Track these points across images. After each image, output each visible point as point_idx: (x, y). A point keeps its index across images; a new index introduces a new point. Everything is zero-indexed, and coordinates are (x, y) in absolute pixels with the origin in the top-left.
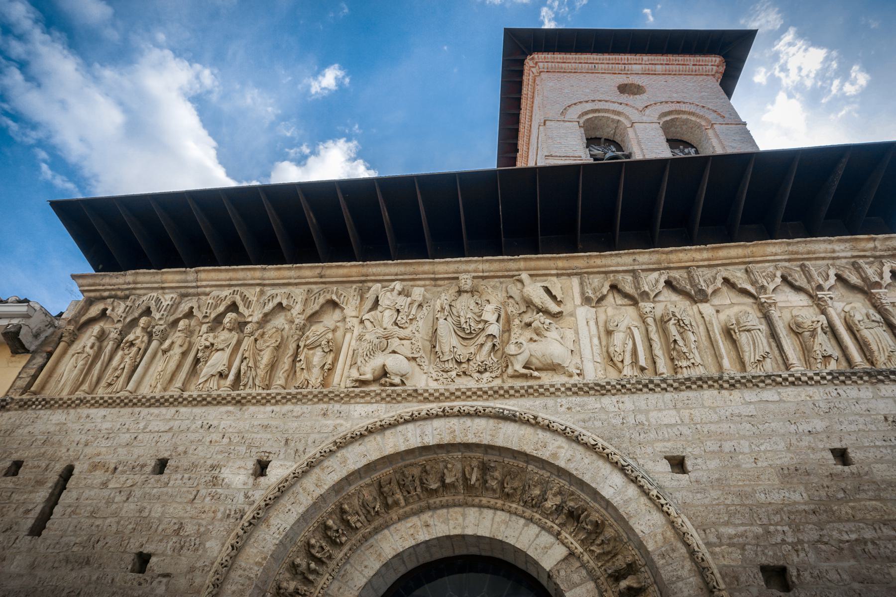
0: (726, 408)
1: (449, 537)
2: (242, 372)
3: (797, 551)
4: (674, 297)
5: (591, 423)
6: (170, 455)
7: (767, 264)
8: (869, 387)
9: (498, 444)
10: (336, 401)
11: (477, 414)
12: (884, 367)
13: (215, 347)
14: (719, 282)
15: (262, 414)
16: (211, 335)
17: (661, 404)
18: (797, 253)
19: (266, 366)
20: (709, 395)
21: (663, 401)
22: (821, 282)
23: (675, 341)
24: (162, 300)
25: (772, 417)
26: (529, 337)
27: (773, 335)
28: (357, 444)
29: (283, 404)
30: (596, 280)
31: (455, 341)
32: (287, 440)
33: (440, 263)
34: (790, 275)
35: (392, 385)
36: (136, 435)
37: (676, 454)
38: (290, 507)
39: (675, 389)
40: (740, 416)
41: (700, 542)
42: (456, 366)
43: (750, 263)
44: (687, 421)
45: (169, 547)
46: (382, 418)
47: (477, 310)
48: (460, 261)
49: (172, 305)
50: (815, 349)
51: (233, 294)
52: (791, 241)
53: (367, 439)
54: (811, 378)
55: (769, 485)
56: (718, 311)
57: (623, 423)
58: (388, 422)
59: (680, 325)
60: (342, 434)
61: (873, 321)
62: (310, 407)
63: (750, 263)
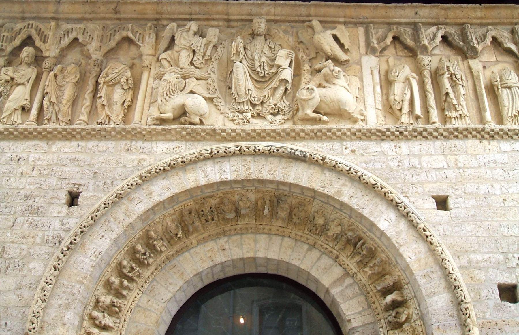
26: (318, 83)
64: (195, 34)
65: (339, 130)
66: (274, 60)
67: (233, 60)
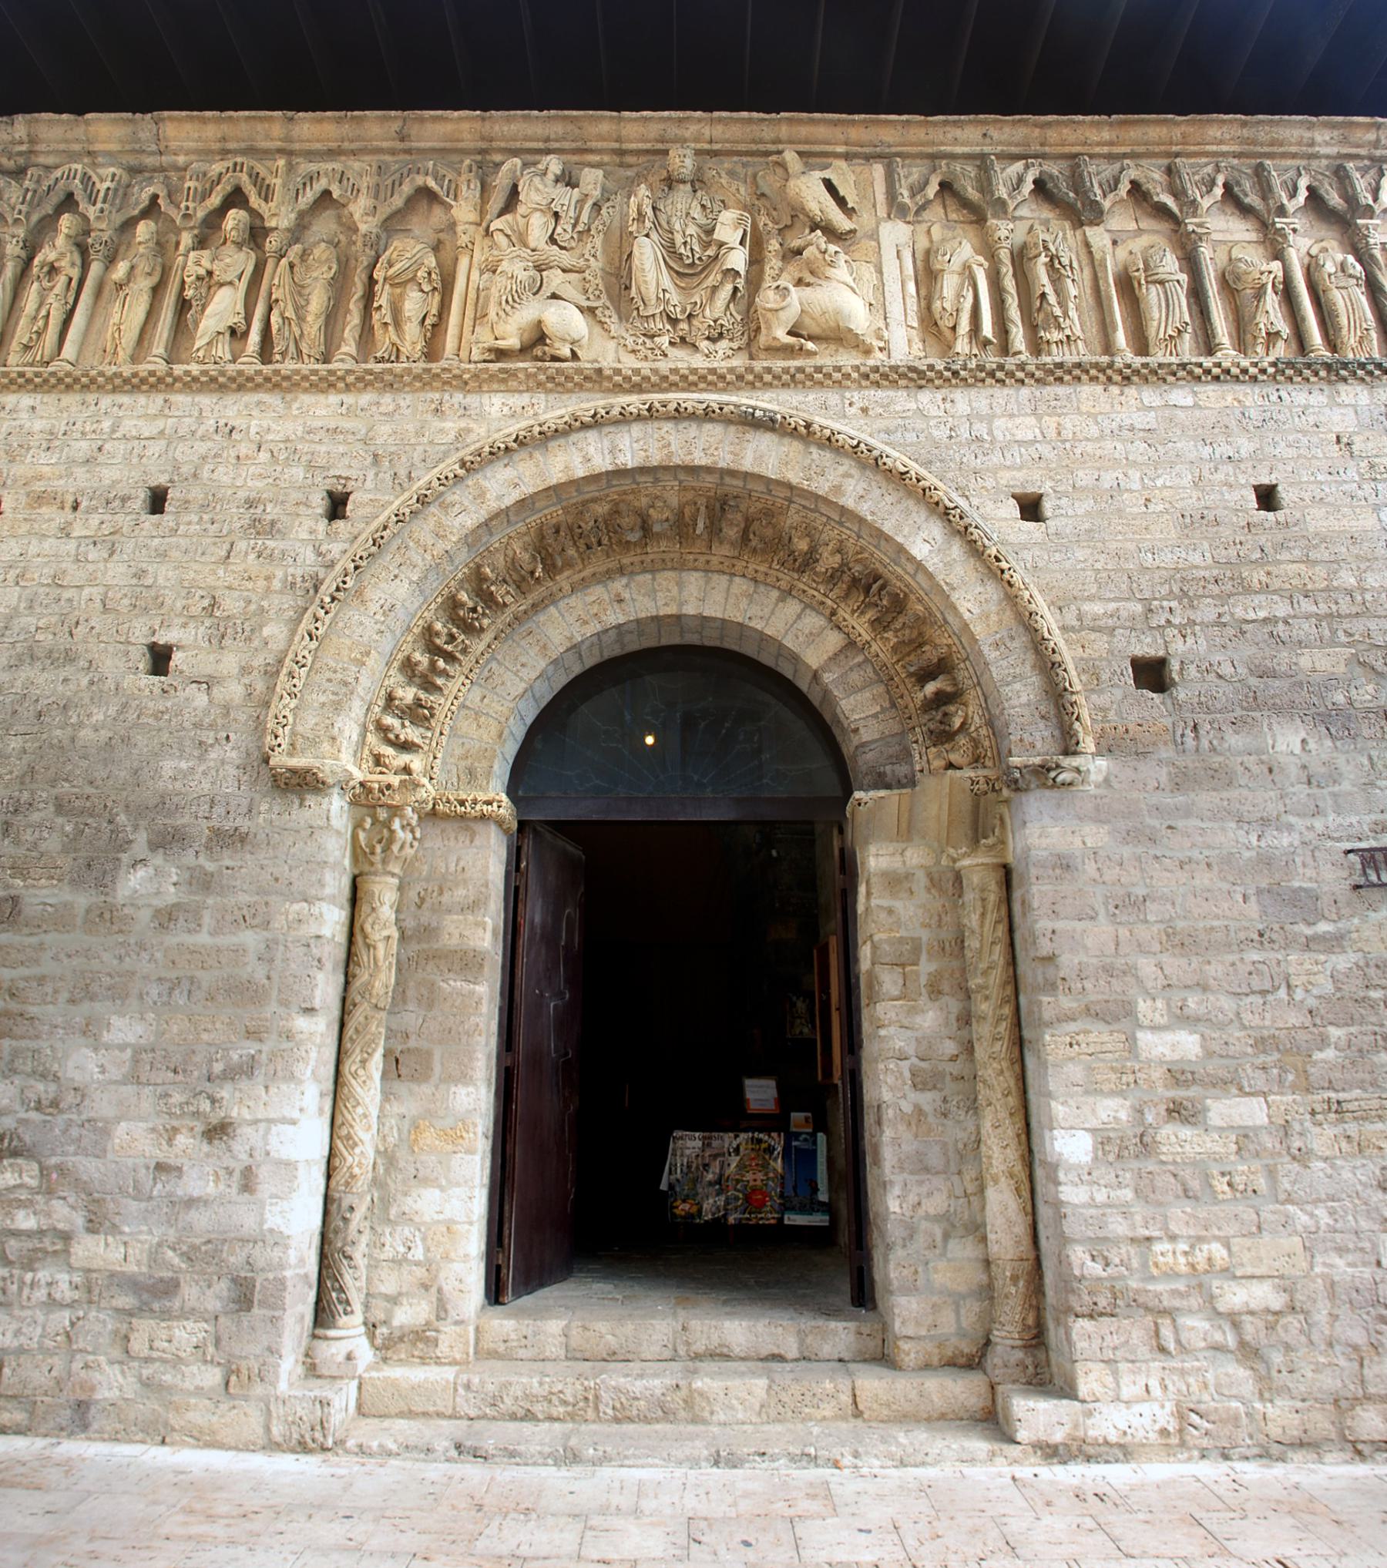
0: (1113, 416)
1: (656, 619)
2: (275, 327)
3: (1184, 637)
4: (1046, 213)
5: (899, 434)
6: (171, 481)
7: (1204, 160)
8: (1325, 387)
9: (744, 469)
10: (457, 388)
11: (708, 415)
12: (1351, 356)
13: (216, 278)
14: (1124, 187)
15: (323, 408)
16: (206, 253)
17: (1013, 407)
18: (1254, 143)
19: (317, 316)
20: (1089, 392)
21: (1017, 401)
22: (1285, 201)
23: (1043, 295)
24: (95, 178)
25: (1179, 433)
26: (797, 275)
27: (1197, 294)
28: (501, 463)
29: (359, 391)
30: (916, 173)
31: (666, 281)
32: (375, 456)
33: (631, 120)
34: (1238, 184)
35: (555, 359)
36: (100, 443)
37: (1030, 490)
38: (396, 572)
39: (1038, 381)
40: (1132, 429)
41: (1054, 626)
42: (668, 327)
43: (1177, 155)
44: (1052, 434)
45: (200, 636)
46: (542, 418)
47: (704, 221)
48: (669, 119)
49: (116, 190)
50: (1258, 319)
51: (234, 171)
52: (1249, 118)
53: (516, 457)
54: (1245, 371)
55: (1160, 540)
56: (1115, 243)
57: (951, 437)
58: (554, 427)
59: (1052, 266)
60: (472, 448)
61: (1350, 276)
62: (409, 397)
63: (1177, 155)
64: (557, 181)
65: (838, 369)
66: (710, 232)
67: (631, 233)
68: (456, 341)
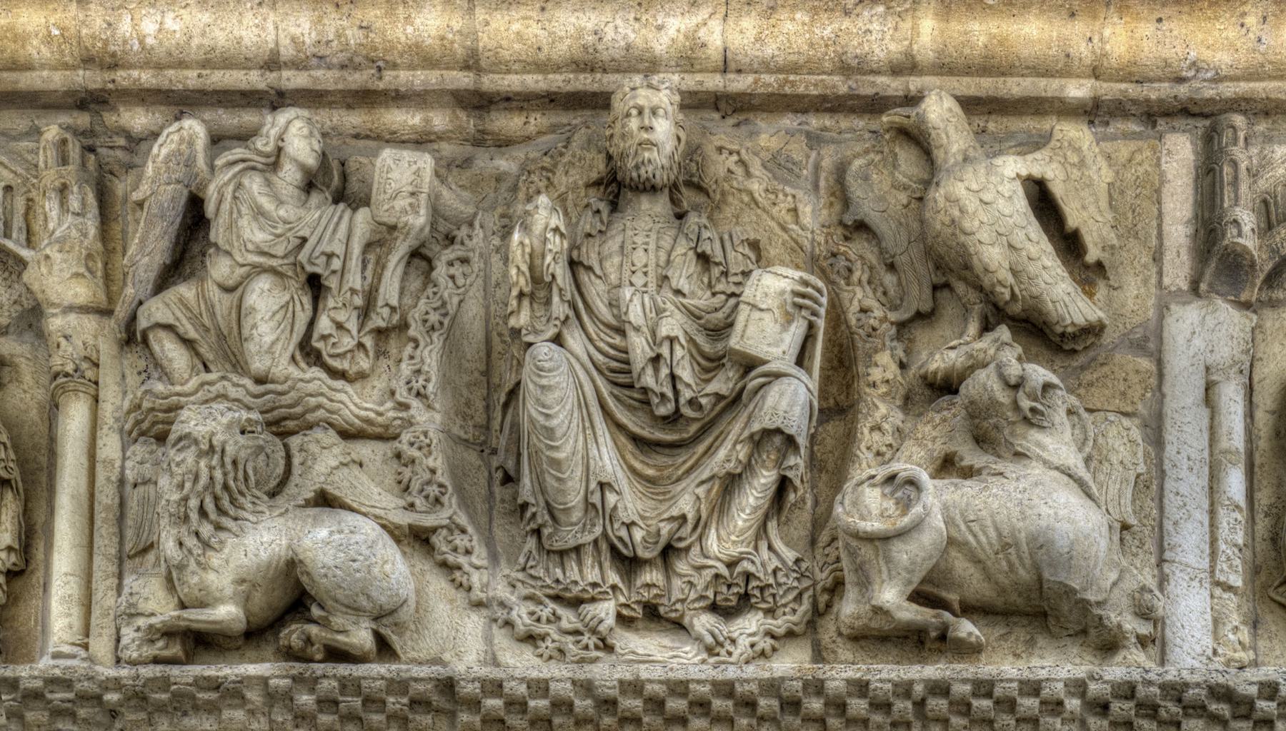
26: (939, 448)
64: (309, 185)
65: (1033, 688)
66: (720, 331)
67: (516, 332)
68: (76, 612)
